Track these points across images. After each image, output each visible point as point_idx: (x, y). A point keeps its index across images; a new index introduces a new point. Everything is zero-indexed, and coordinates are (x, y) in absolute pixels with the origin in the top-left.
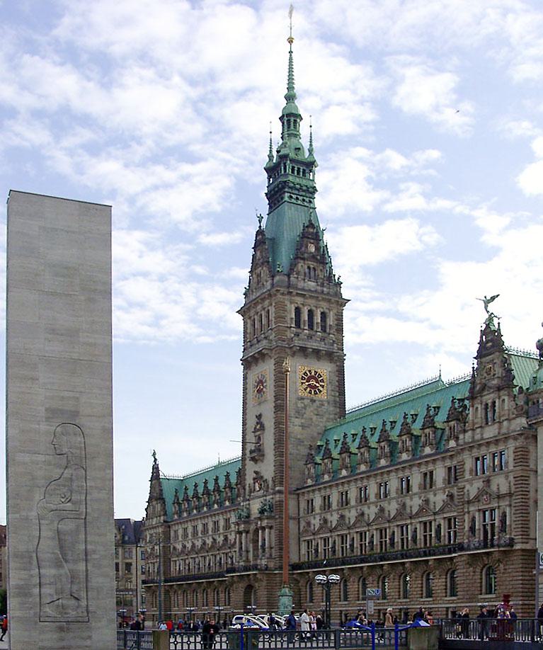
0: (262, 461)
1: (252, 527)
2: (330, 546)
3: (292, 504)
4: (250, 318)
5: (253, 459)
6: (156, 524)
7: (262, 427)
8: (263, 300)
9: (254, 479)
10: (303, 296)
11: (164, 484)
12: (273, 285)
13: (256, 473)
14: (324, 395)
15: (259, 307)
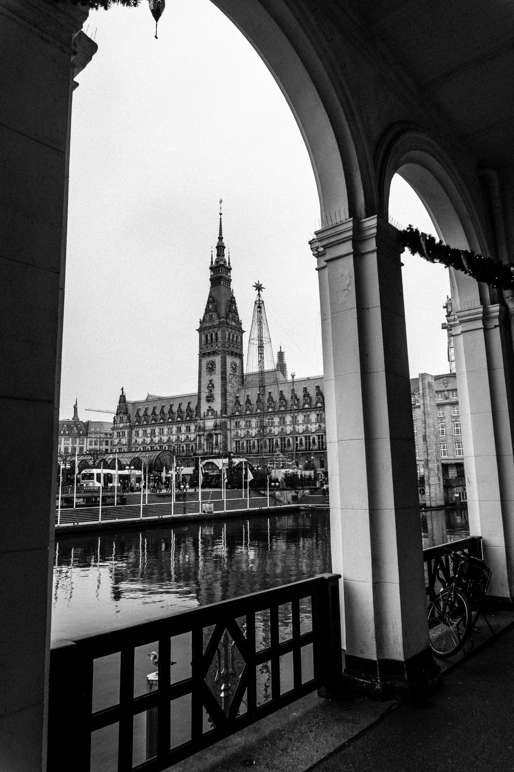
0: (213, 402)
1: (206, 433)
2: (251, 444)
3: (228, 423)
4: (204, 334)
5: (208, 401)
6: (124, 427)
7: (213, 386)
8: (214, 328)
9: (208, 410)
10: (230, 328)
11: (130, 408)
12: (220, 322)
13: (210, 407)
14: (238, 373)
15: (211, 330)
